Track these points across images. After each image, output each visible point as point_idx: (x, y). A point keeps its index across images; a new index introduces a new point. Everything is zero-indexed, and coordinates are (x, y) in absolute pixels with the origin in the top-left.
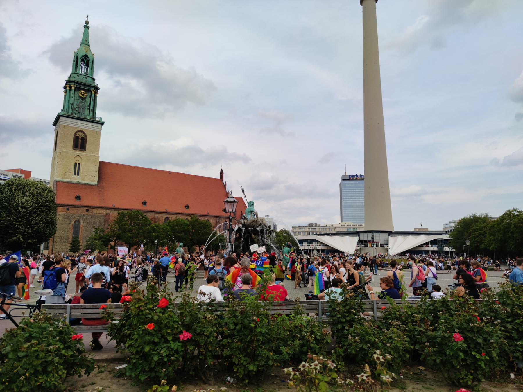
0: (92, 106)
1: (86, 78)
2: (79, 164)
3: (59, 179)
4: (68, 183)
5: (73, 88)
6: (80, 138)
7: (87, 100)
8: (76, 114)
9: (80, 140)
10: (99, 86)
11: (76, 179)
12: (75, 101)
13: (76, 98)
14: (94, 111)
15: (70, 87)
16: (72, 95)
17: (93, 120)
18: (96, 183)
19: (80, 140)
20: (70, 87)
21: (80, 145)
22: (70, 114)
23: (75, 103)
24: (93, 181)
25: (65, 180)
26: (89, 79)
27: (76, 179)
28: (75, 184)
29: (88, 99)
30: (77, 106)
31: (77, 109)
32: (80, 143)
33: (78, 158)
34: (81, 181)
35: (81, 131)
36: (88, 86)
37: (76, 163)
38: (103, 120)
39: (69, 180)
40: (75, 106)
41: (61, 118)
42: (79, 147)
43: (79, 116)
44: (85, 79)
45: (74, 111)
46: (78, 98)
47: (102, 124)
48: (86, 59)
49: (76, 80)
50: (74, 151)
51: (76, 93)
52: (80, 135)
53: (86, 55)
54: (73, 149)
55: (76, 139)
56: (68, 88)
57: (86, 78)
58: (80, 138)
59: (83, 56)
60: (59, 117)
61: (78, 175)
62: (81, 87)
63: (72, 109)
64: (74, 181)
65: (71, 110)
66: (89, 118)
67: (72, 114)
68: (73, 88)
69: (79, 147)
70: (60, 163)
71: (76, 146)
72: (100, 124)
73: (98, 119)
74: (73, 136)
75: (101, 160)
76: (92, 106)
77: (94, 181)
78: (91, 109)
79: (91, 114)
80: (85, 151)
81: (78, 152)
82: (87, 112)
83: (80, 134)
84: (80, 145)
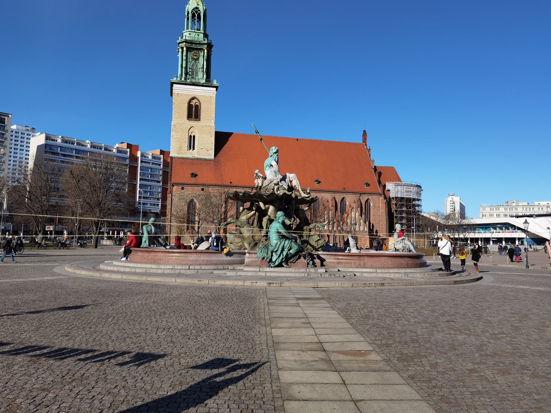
1: (198, 35)
2: (194, 136)
4: (183, 158)
5: (185, 49)
6: (194, 106)
7: (200, 61)
9: (194, 109)
10: (212, 43)
13: (188, 61)
15: (182, 48)
16: (184, 58)
18: (212, 157)
19: (194, 109)
20: (182, 48)
21: (193, 114)
22: (183, 79)
23: (188, 66)
24: (209, 155)
25: (180, 156)
26: (201, 36)
27: (191, 154)
29: (201, 59)
30: (191, 70)
31: (190, 73)
34: (197, 156)
35: (193, 98)
36: (200, 44)
41: (174, 85)
42: (193, 117)
43: (194, 81)
44: (197, 36)
46: (191, 60)
48: (197, 12)
49: (187, 38)
51: (189, 54)
52: (193, 103)
53: (197, 8)
55: (190, 107)
56: (180, 50)
57: (198, 35)
58: (194, 106)
59: (194, 9)
61: (194, 149)
62: (194, 46)
64: (190, 156)
65: (184, 75)
67: (185, 79)
68: (185, 49)
69: (193, 117)
71: (189, 117)
76: (205, 67)
77: (210, 155)
82: (200, 75)
83: (194, 101)
84: (193, 114)
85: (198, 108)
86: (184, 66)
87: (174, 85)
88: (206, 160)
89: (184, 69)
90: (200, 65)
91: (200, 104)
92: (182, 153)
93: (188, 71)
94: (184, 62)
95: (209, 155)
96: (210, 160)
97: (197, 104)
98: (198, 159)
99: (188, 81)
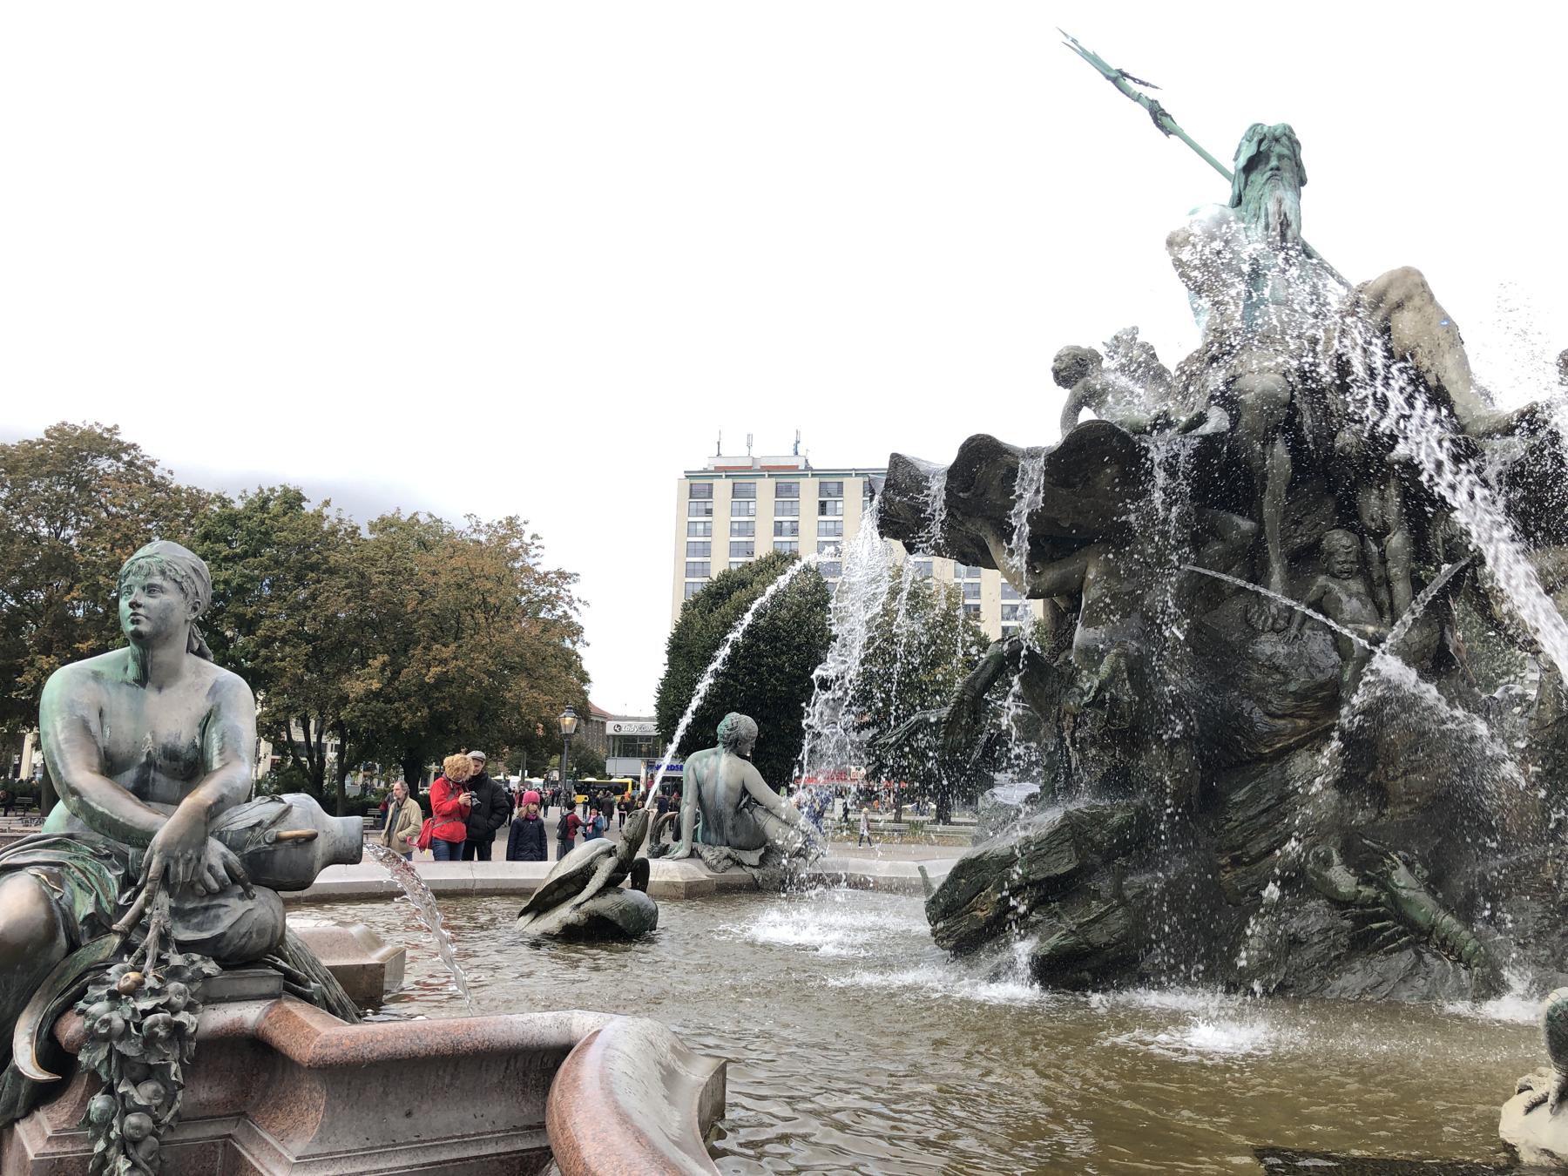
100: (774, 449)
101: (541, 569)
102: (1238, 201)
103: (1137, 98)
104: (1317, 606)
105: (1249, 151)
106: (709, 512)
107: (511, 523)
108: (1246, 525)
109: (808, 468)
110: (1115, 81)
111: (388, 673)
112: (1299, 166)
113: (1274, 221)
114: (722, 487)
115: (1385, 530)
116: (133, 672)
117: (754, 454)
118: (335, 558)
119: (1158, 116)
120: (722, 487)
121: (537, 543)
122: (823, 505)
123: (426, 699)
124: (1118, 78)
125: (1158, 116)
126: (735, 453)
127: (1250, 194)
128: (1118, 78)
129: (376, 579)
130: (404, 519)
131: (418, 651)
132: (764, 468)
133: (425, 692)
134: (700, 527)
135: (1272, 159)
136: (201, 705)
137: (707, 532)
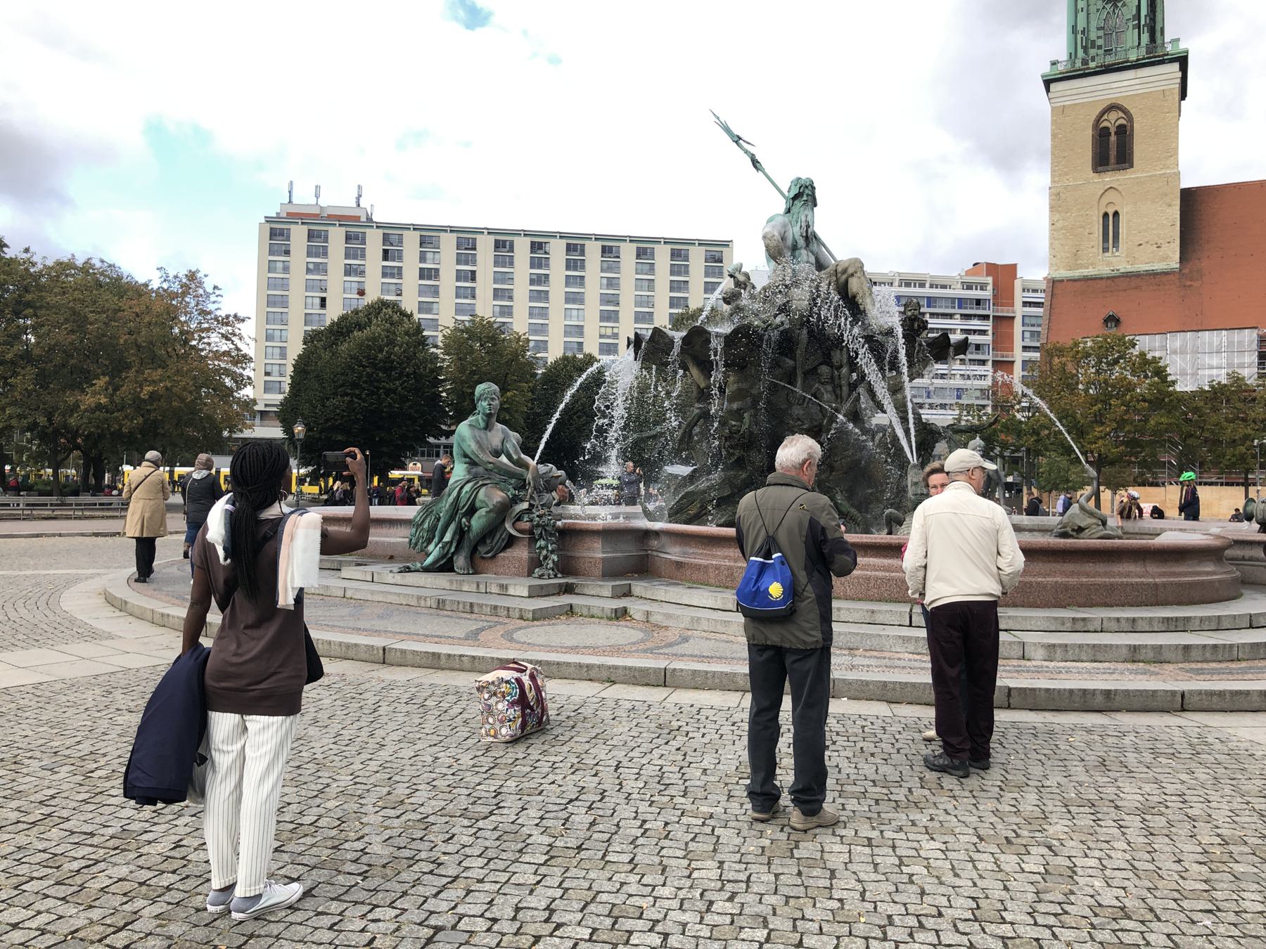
0: (1144, 12)
2: (1116, 214)
3: (1063, 273)
4: (1086, 279)
6: (1113, 130)
8: (1093, 60)
9: (1113, 138)
11: (1109, 264)
12: (1092, 16)
13: (1093, 9)
14: (1153, 27)
17: (1155, 58)
18: (1174, 263)
19: (1113, 138)
21: (1113, 153)
22: (1078, 64)
24: (1165, 258)
25: (1077, 273)
27: (1109, 264)
28: (1108, 278)
30: (1101, 33)
31: (1100, 42)
32: (1113, 146)
33: (1111, 196)
34: (1124, 267)
35: (1113, 107)
37: (1106, 215)
38: (1182, 46)
39: (1090, 272)
40: (1093, 36)
42: (1112, 159)
43: (1109, 60)
45: (1092, 52)
47: (1183, 61)
50: (1096, 178)
54: (1095, 170)
55: (1101, 135)
58: (1113, 130)
60: (1048, 83)
63: (1085, 49)
64: (1104, 270)
65: (1080, 53)
66: (1133, 57)
67: (1085, 62)
69: (1112, 159)
70: (1059, 225)
72: (1172, 61)
73: (1169, 48)
74: (1089, 133)
75: (1185, 184)
76: (1144, 12)
77: (1170, 258)
78: (1143, 22)
79: (1145, 38)
80: (1132, 166)
81: (1109, 178)
82: (1131, 36)
83: (1113, 116)
84: (1113, 153)
85: (1125, 133)
86: (1080, 28)
87: (1053, 86)
88: (1153, 274)
89: (1079, 36)
90: (1129, 12)
91: (1130, 118)
92: (1082, 266)
93: (1093, 36)
94: (1082, 16)
95: (1165, 258)
96: (1165, 273)
97: (1122, 122)
98: (1128, 276)
99: (1092, 65)
100: (337, 198)
101: (222, 313)
102: (788, 211)
103: (746, 152)
104: (814, 395)
105: (795, 191)
106: (287, 253)
107: (192, 276)
108: (791, 362)
109: (369, 219)
110: (736, 142)
111: (110, 390)
112: (815, 199)
113: (804, 225)
114: (299, 234)
115: (841, 366)
116: (482, 425)
117: (322, 203)
118: (51, 299)
119: (755, 163)
120: (299, 234)
121: (217, 292)
122: (386, 252)
123: (138, 409)
124: (737, 140)
125: (755, 163)
126: (304, 198)
127: (794, 210)
128: (737, 140)
129: (92, 317)
130: (80, 262)
131: (132, 373)
132: (330, 217)
133: (138, 404)
134: (280, 265)
135: (804, 195)
136: (501, 436)
137: (286, 269)
